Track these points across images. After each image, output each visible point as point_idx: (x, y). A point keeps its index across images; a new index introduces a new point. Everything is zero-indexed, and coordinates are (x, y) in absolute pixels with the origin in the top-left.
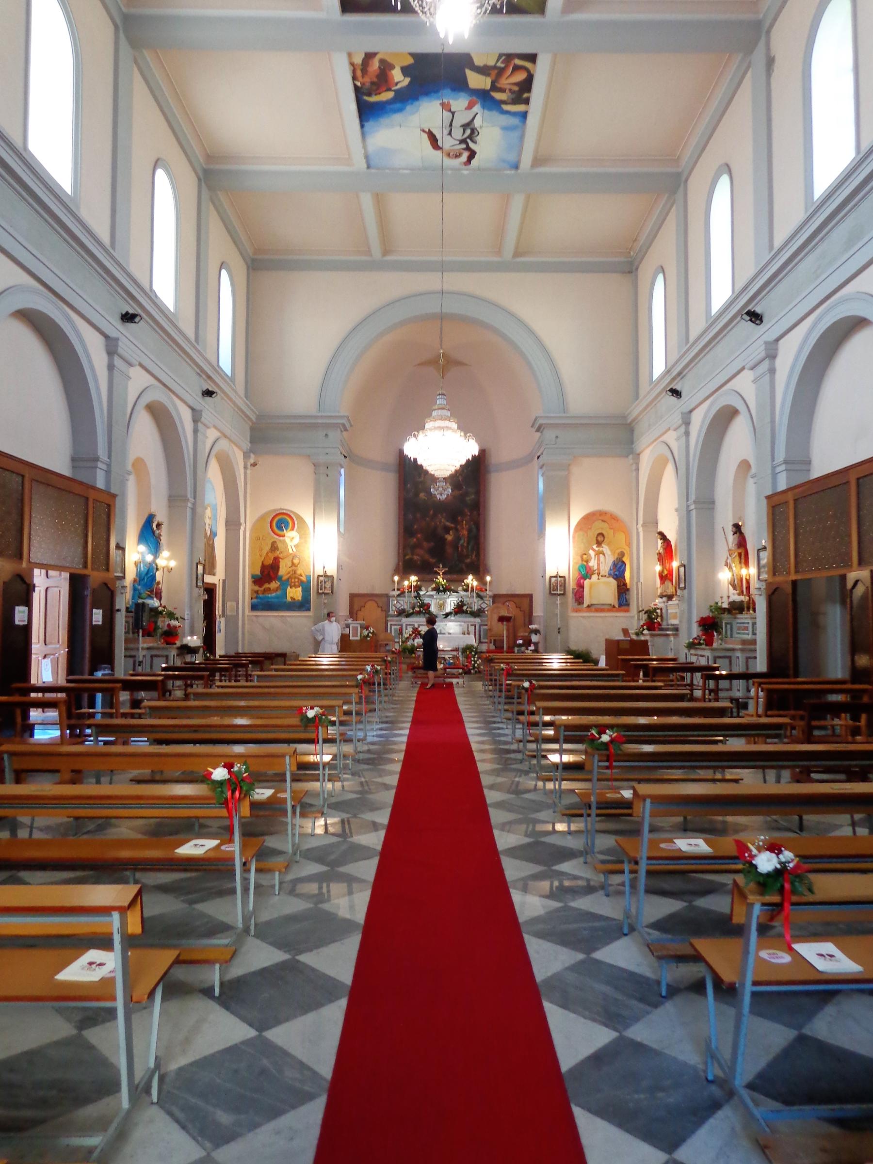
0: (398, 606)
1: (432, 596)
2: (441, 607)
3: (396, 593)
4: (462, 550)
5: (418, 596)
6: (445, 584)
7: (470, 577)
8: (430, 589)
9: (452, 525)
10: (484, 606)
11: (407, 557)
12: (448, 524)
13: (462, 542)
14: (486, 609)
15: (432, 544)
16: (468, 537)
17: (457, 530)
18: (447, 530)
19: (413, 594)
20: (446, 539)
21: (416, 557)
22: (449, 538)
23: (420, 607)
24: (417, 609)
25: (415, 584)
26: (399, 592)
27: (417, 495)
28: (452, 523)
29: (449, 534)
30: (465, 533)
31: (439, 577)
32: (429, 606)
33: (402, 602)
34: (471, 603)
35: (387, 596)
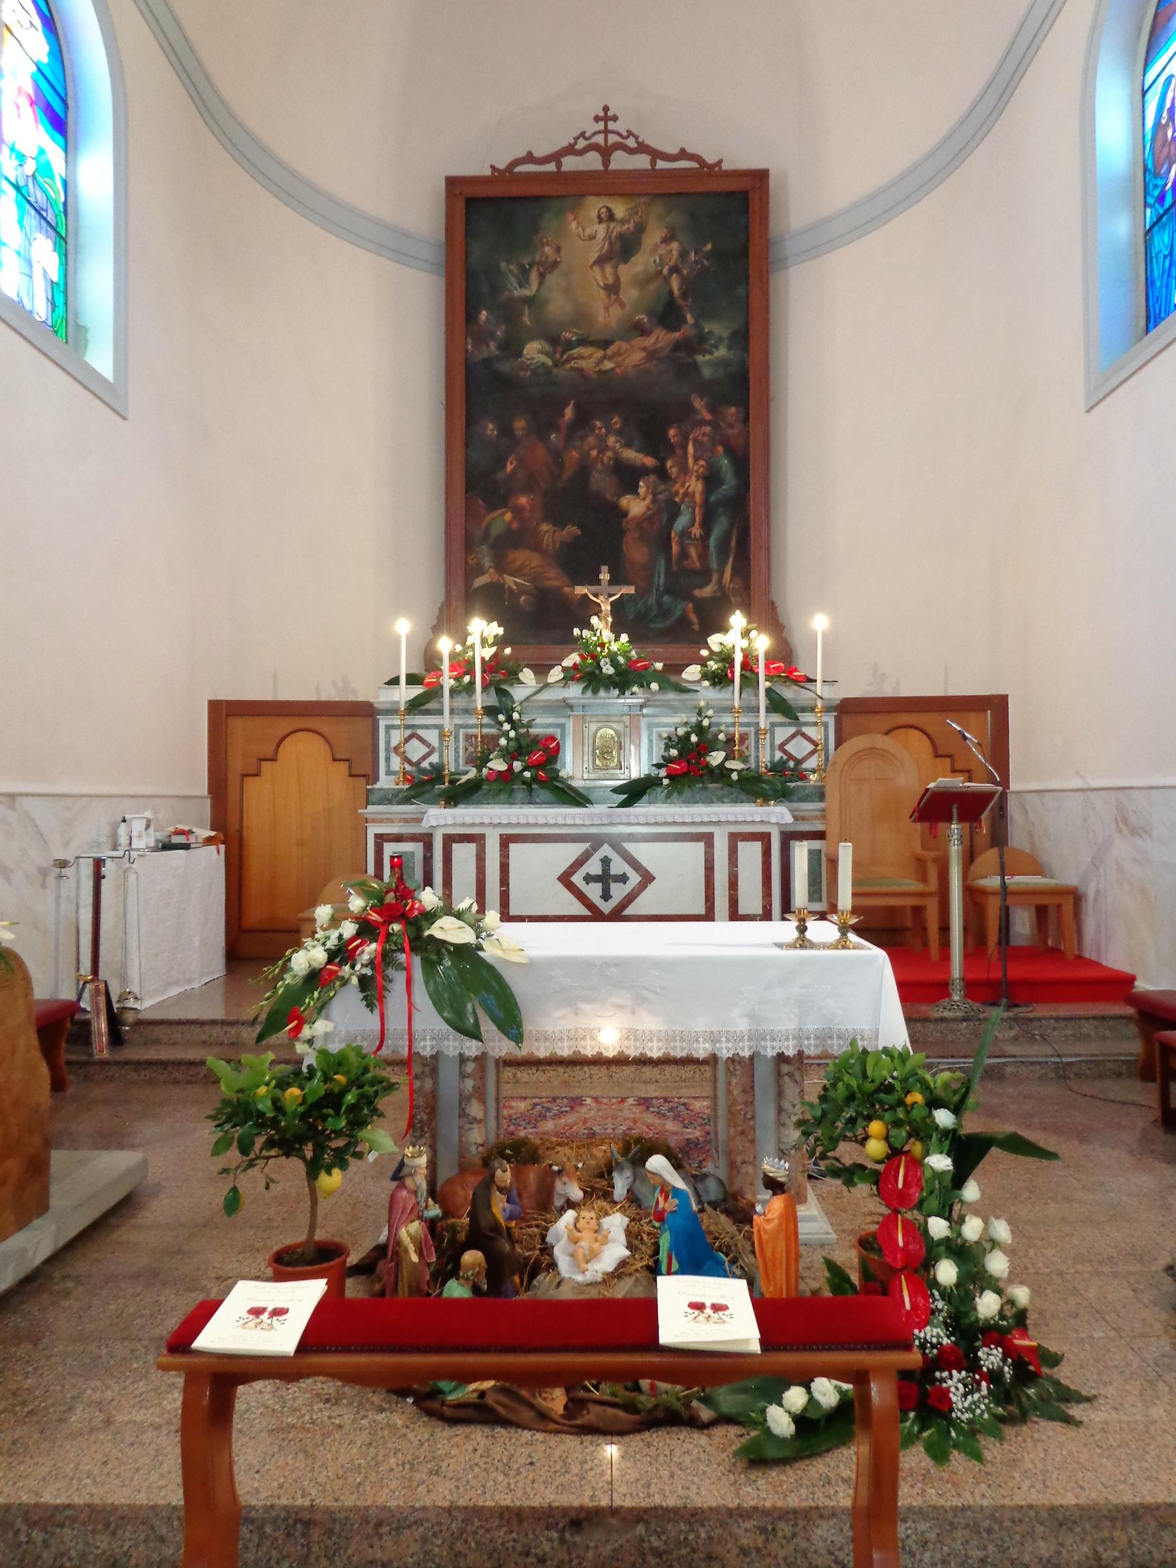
0: (416, 750)
1: (566, 706)
2: (605, 753)
3: (405, 693)
4: (684, 554)
5: (500, 709)
6: (625, 654)
7: (738, 620)
8: (556, 674)
9: (649, 461)
10: (798, 748)
11: (480, 581)
12: (631, 455)
13: (681, 522)
14: (811, 763)
15: (572, 530)
16: (706, 501)
17: (662, 473)
18: (628, 477)
19: (480, 699)
20: (625, 514)
21: (510, 581)
22: (636, 506)
23: (510, 755)
24: (499, 765)
25: (488, 653)
26: (417, 690)
27: (512, 347)
28: (647, 454)
29: (634, 490)
30: (695, 486)
31: (594, 620)
32: (550, 751)
33: (432, 737)
34: (744, 738)
35: (366, 712)
